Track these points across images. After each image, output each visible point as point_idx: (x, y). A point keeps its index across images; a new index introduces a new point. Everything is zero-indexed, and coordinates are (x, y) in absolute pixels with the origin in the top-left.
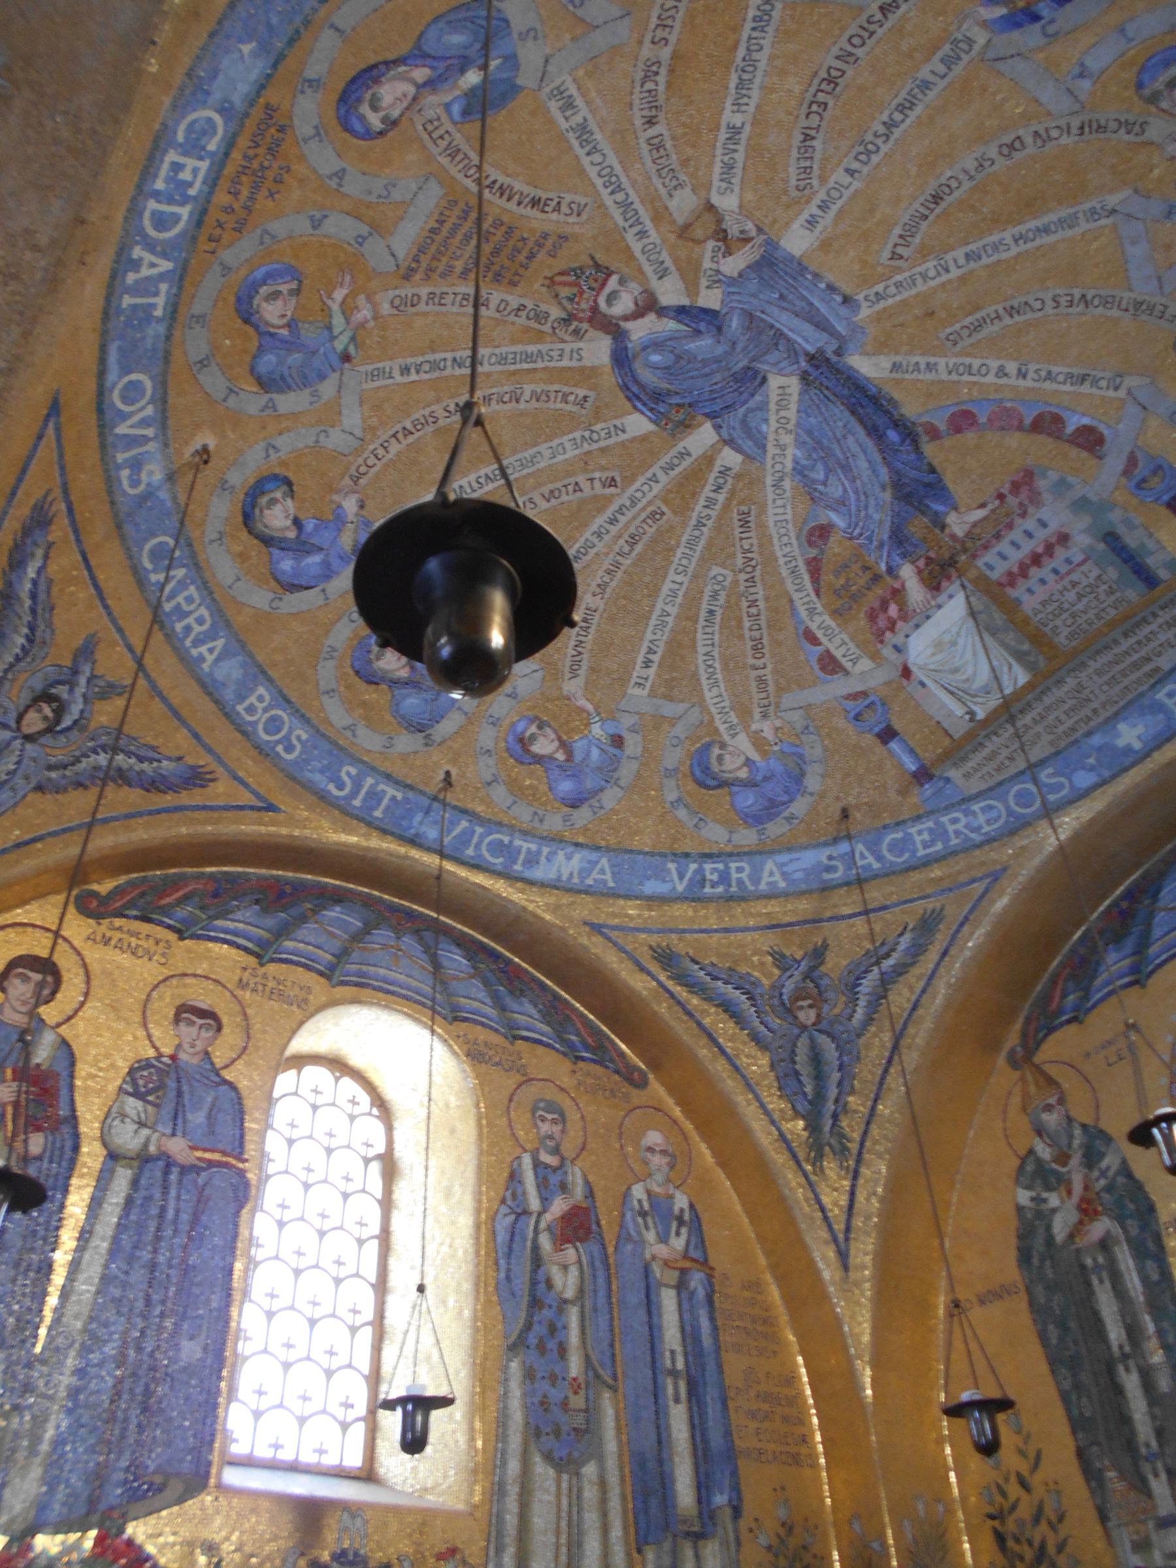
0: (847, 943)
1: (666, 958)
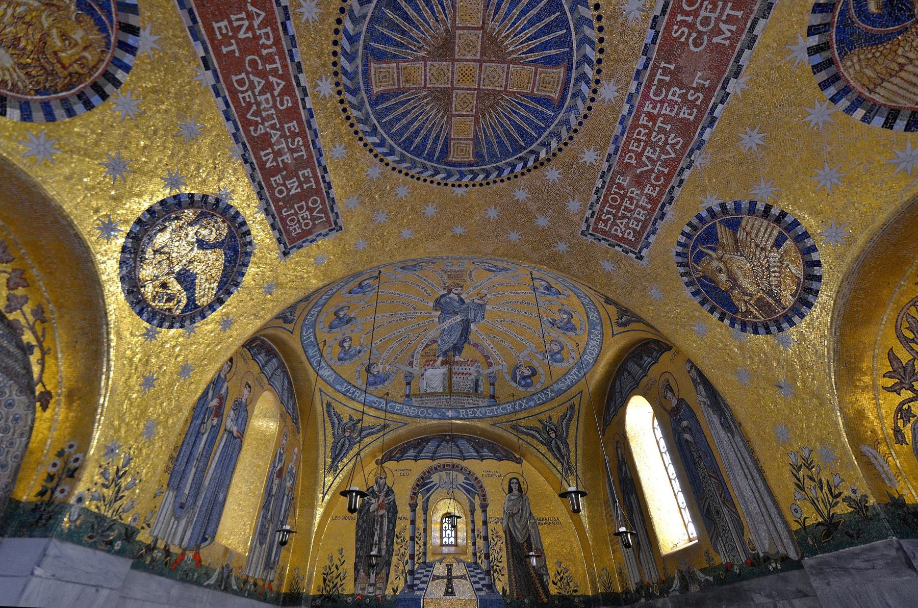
0: (367, 421)
1: (329, 405)
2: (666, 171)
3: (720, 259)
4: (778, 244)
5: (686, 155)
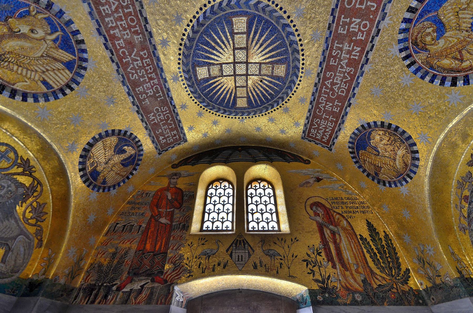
2: (124, 61)
3: (44, 39)
4: (45, 82)
5: (124, 74)
